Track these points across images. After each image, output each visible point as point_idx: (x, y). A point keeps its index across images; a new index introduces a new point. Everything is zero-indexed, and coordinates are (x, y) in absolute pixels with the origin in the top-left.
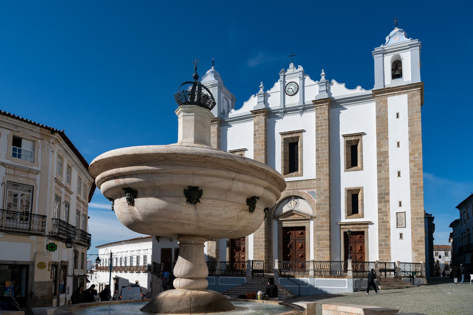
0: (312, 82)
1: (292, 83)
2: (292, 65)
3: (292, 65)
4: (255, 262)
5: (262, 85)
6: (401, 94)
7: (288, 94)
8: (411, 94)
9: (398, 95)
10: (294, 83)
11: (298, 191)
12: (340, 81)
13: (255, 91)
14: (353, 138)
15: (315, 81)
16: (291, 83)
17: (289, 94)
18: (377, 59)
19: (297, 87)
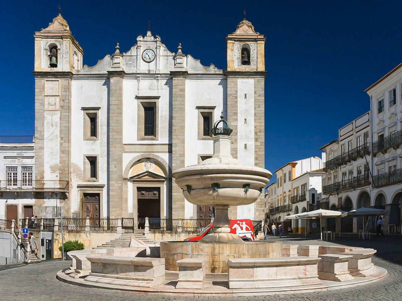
0: (169, 53)
1: (150, 50)
2: (149, 33)
3: (149, 33)
4: (125, 220)
5: (118, 47)
6: (249, 79)
7: (145, 60)
8: (257, 80)
9: (246, 79)
10: (151, 51)
11: (154, 154)
12: (195, 57)
13: (111, 53)
14: (206, 111)
15: (172, 52)
16: (148, 50)
17: (146, 60)
18: (230, 44)
19: (154, 55)
